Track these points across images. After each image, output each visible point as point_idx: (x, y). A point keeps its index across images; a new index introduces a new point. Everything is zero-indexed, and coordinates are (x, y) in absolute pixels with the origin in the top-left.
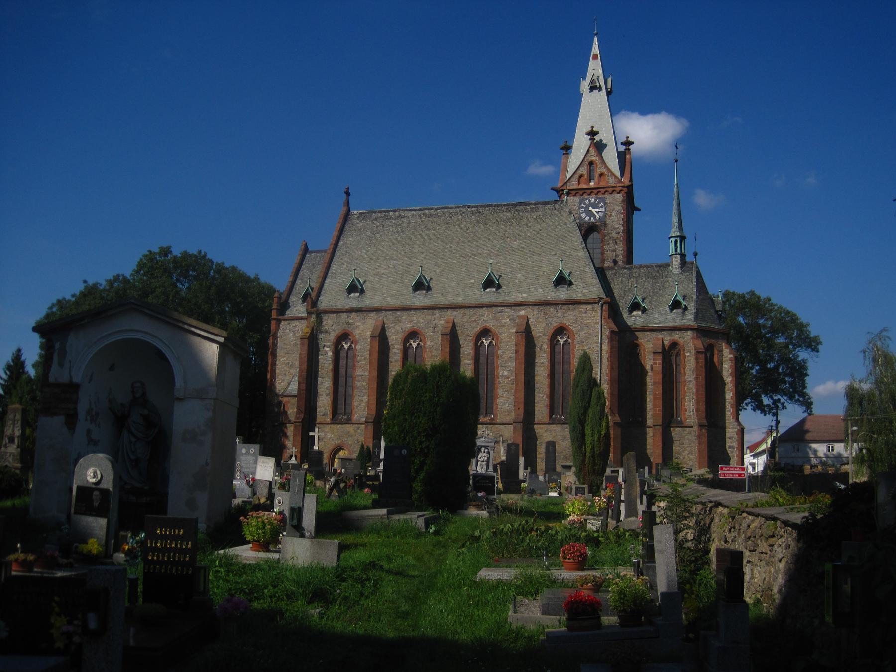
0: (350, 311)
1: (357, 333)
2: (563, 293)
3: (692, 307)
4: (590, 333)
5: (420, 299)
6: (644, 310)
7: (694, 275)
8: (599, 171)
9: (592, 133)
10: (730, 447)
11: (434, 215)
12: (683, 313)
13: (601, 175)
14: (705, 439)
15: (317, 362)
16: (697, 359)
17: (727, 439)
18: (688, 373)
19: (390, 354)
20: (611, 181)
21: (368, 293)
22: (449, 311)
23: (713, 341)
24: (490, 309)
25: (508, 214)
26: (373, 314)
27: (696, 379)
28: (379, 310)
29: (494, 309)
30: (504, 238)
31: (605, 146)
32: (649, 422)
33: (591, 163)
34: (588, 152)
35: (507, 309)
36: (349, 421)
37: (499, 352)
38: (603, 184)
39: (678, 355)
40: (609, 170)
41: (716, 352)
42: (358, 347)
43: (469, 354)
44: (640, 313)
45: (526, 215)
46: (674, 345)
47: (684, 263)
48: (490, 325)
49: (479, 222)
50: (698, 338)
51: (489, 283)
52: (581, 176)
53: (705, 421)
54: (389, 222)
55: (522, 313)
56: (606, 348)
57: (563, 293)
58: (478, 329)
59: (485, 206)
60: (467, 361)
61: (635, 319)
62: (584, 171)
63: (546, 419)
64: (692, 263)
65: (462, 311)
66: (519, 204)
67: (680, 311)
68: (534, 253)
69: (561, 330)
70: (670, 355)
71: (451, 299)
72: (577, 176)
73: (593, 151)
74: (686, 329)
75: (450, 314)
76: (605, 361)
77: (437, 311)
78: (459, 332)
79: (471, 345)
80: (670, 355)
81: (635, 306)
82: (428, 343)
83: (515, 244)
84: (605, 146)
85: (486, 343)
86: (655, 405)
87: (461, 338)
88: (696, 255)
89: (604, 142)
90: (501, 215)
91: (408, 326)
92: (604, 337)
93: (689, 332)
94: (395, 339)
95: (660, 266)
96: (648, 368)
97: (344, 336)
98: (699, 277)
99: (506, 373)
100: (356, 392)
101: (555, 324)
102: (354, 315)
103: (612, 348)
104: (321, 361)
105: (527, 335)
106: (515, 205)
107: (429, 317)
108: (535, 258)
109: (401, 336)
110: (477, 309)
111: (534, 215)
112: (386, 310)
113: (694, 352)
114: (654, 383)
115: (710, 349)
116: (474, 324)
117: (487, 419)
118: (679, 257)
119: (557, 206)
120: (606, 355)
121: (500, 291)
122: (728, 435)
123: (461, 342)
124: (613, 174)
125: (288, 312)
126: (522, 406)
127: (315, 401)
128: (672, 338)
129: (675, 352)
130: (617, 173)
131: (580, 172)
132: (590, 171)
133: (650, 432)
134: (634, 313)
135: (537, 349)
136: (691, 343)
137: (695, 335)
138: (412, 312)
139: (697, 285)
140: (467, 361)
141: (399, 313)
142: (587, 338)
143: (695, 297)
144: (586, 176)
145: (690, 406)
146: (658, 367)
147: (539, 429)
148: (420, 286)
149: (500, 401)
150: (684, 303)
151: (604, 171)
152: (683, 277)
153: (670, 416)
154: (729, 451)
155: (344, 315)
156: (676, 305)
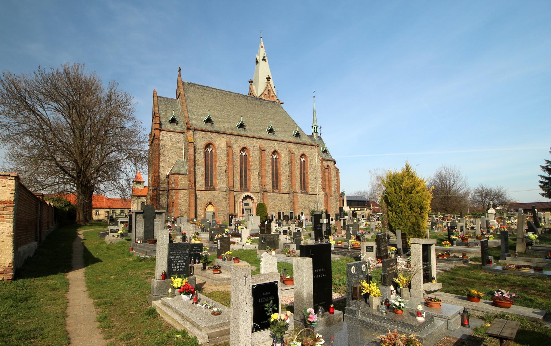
1: (216, 144)
9: (268, 79)
18: (332, 177)
22: (260, 140)
33: (269, 91)
35: (283, 143)
36: (214, 190)
42: (218, 152)
48: (277, 149)
54: (206, 92)
58: (272, 150)
62: (266, 93)
65: (265, 141)
69: (303, 155)
72: (264, 94)
77: (255, 139)
82: (251, 154)
83: (269, 116)
88: (321, 134)
91: (242, 145)
97: (208, 145)
100: (218, 175)
101: (301, 153)
109: (239, 149)
125: (163, 126)
141: (237, 137)
148: (242, 126)
149: (282, 183)
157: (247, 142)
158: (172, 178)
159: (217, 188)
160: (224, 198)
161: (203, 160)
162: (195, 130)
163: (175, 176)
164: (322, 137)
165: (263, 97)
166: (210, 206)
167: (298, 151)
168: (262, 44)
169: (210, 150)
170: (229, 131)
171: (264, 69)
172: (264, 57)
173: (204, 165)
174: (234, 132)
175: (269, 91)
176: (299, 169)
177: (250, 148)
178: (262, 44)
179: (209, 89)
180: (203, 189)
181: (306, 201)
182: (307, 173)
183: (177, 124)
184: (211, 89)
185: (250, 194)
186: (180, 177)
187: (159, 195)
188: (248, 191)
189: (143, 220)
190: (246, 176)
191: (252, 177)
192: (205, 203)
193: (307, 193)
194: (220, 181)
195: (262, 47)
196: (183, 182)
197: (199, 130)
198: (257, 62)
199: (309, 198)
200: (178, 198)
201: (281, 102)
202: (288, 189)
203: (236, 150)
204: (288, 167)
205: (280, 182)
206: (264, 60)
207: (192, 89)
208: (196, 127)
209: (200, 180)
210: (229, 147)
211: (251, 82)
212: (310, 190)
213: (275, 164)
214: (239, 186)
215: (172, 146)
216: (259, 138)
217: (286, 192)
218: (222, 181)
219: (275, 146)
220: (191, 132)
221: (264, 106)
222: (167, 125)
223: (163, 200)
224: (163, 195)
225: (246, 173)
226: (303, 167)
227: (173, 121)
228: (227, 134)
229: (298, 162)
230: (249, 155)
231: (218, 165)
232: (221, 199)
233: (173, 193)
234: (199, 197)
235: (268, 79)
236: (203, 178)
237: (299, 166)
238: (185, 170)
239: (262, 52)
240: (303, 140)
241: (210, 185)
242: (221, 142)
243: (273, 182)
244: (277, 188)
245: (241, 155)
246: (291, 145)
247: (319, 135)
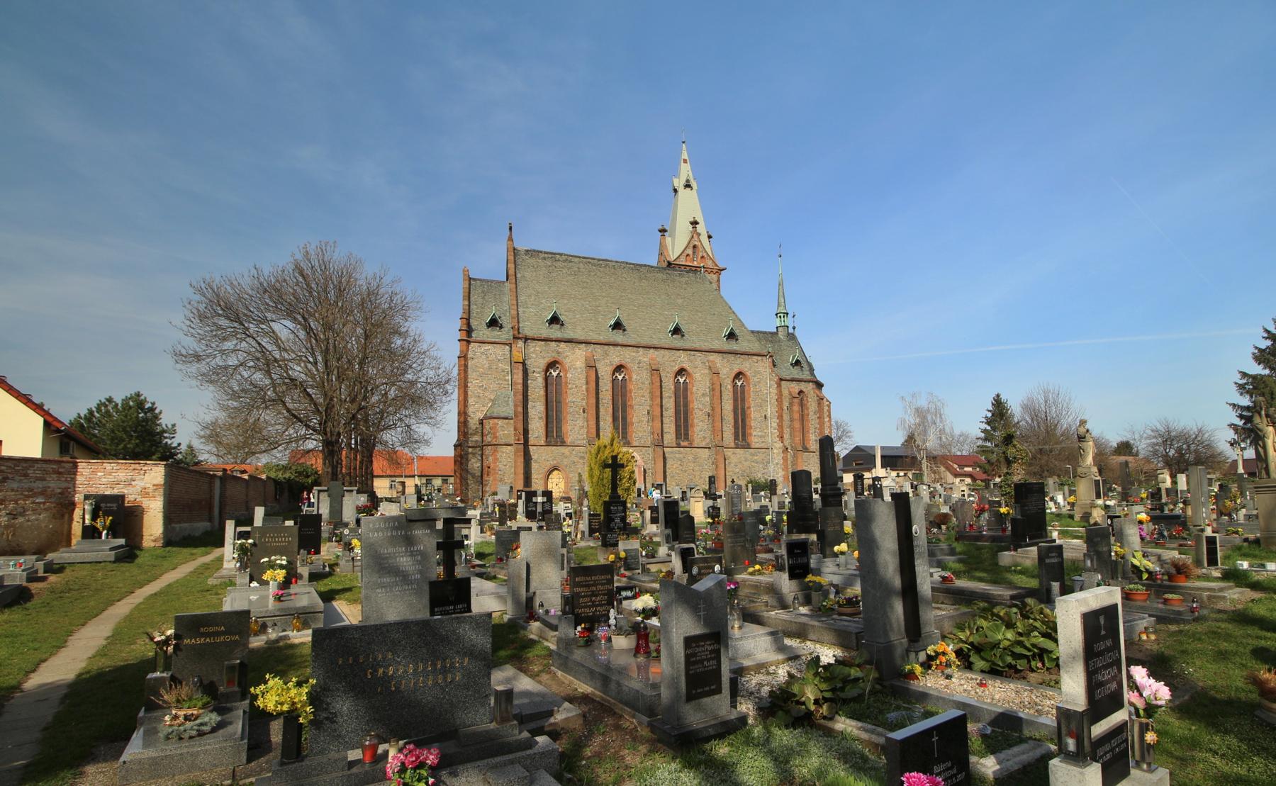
1: (567, 362)
2: (733, 346)
5: (618, 337)
9: (695, 223)
33: (695, 247)
36: (563, 444)
42: (569, 375)
46: (801, 392)
48: (686, 366)
51: (677, 331)
54: (558, 264)
57: (733, 346)
58: (676, 368)
62: (690, 251)
63: (733, 445)
69: (739, 375)
83: (680, 301)
91: (616, 362)
94: (605, 371)
95: (772, 333)
97: (552, 365)
100: (569, 417)
101: (736, 370)
102: (562, 345)
109: (610, 369)
111: (684, 279)
117: (686, 444)
125: (474, 335)
148: (618, 326)
149: (697, 429)
157: (625, 356)
158: (488, 424)
159: (569, 441)
160: (582, 458)
161: (542, 393)
162: (526, 339)
163: (492, 421)
164: (797, 334)
165: (682, 261)
166: (556, 472)
167: (727, 367)
168: (685, 155)
169: (555, 374)
170: (593, 337)
171: (688, 205)
172: (688, 181)
173: (543, 400)
174: (601, 339)
175: (695, 247)
176: (731, 402)
177: (633, 367)
178: (685, 155)
179: (564, 258)
180: (542, 442)
183: (501, 327)
184: (569, 258)
186: (500, 422)
187: (467, 453)
189: (328, 499)
190: (624, 419)
191: (635, 419)
193: (748, 447)
194: (575, 427)
195: (685, 161)
196: (506, 431)
197: (534, 339)
198: (675, 191)
199: (752, 455)
200: (496, 460)
201: (721, 266)
202: (708, 440)
203: (605, 371)
204: (708, 399)
205: (692, 426)
206: (688, 186)
207: (532, 261)
208: (529, 333)
210: (591, 366)
211: (663, 231)
212: (755, 440)
213: (682, 395)
215: (490, 368)
217: (703, 444)
218: (577, 429)
219: (683, 360)
220: (520, 344)
221: (674, 281)
222: (481, 332)
223: (474, 464)
224: (474, 454)
225: (624, 411)
226: (740, 398)
227: (493, 323)
228: (588, 343)
229: (730, 387)
230: (631, 378)
231: (570, 398)
232: (576, 459)
233: (488, 450)
234: (534, 457)
235: (695, 223)
236: (543, 424)
237: (731, 394)
238: (509, 410)
239: (685, 171)
240: (743, 345)
241: (554, 435)
242: (575, 359)
243: (677, 426)
244: (687, 438)
245: (614, 381)
246: (713, 357)
247: (791, 331)
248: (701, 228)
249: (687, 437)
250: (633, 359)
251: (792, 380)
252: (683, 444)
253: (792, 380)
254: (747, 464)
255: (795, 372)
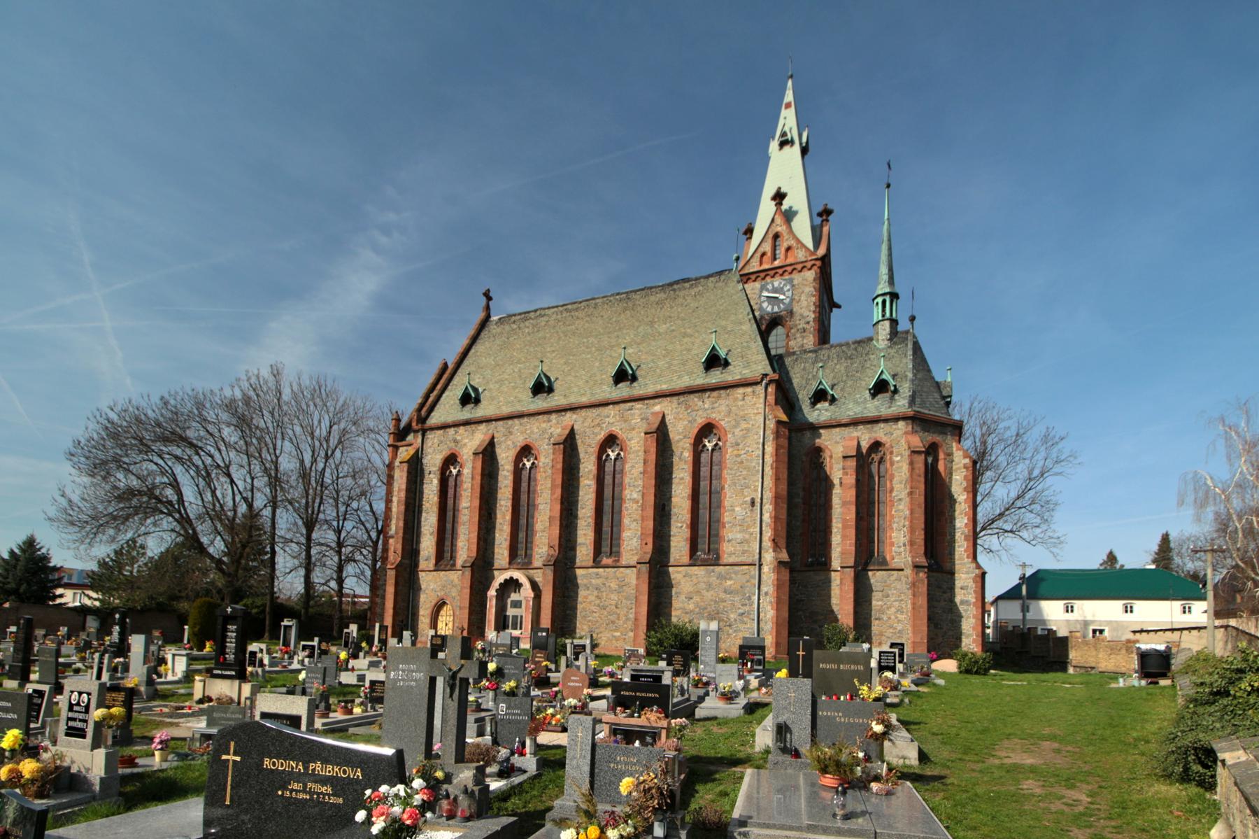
0: (456, 425)
3: (905, 389)
4: (748, 430)
6: (833, 400)
7: (910, 346)
8: (785, 245)
10: (962, 602)
11: (577, 309)
12: (892, 399)
13: (788, 249)
14: (923, 589)
15: (422, 493)
16: (911, 463)
17: (957, 590)
19: (500, 478)
20: (801, 255)
21: (484, 402)
22: (569, 414)
23: (937, 438)
24: (617, 407)
25: (662, 295)
26: (483, 427)
27: (911, 494)
28: (488, 420)
29: (622, 405)
30: (652, 323)
31: (796, 213)
32: (836, 563)
33: (776, 236)
34: (773, 220)
35: (638, 405)
37: (627, 466)
38: (790, 261)
39: (881, 461)
40: (798, 241)
41: (941, 456)
43: (590, 471)
44: (826, 404)
45: (682, 293)
46: (876, 446)
47: (894, 333)
48: (616, 429)
49: (625, 309)
50: (914, 432)
52: (764, 254)
53: (922, 560)
55: (657, 408)
56: (770, 449)
58: (602, 436)
59: (635, 291)
60: (587, 482)
61: (818, 414)
62: (767, 247)
63: (686, 559)
64: (907, 332)
65: (584, 413)
66: (677, 282)
67: (888, 395)
68: (685, 335)
69: (708, 429)
70: (867, 462)
71: (574, 399)
73: (779, 220)
74: (896, 419)
75: (569, 418)
76: (768, 470)
77: (554, 416)
78: (579, 442)
79: (593, 459)
80: (867, 462)
81: (820, 396)
83: (663, 328)
84: (796, 213)
85: (613, 455)
86: (844, 537)
87: (581, 449)
89: (794, 209)
90: (652, 298)
91: (520, 440)
92: (768, 432)
93: (901, 424)
94: (506, 458)
95: (859, 342)
96: (836, 481)
98: (917, 348)
99: (635, 496)
101: (701, 421)
102: (462, 429)
103: (778, 448)
104: (426, 491)
105: (661, 435)
106: (671, 284)
107: (544, 425)
108: (685, 340)
110: (601, 409)
112: (496, 420)
113: (907, 453)
114: (844, 504)
115: (932, 450)
116: (597, 430)
118: (887, 324)
119: (723, 277)
120: (769, 459)
121: (635, 384)
122: (958, 584)
123: (581, 456)
124: (803, 246)
126: (650, 540)
127: (418, 542)
128: (874, 435)
129: (876, 457)
130: (810, 245)
131: (761, 250)
132: (774, 248)
133: (836, 578)
134: (819, 406)
135: (675, 459)
136: (903, 442)
137: (910, 428)
138: (526, 419)
139: (914, 360)
140: (587, 482)
141: (510, 422)
142: (744, 437)
143: (910, 375)
144: (769, 254)
145: (900, 536)
146: (851, 479)
147: (676, 574)
150: (892, 382)
151: (793, 243)
152: (892, 351)
153: (867, 554)
154: (961, 608)
155: (451, 431)
156: (880, 387)
174: (506, 410)
181: (709, 587)
182: (723, 488)
185: (517, 574)
188: (526, 565)
192: (434, 602)
199: (721, 577)
209: (428, 545)
214: (506, 553)
216: (565, 410)
228: (488, 420)
229: (688, 455)
245: (517, 472)
246: (658, 407)
248: (797, 199)
249: (615, 552)
250: (544, 431)
251: (855, 423)
252: (605, 561)
253: (855, 423)
254: (709, 595)
255: (878, 406)
